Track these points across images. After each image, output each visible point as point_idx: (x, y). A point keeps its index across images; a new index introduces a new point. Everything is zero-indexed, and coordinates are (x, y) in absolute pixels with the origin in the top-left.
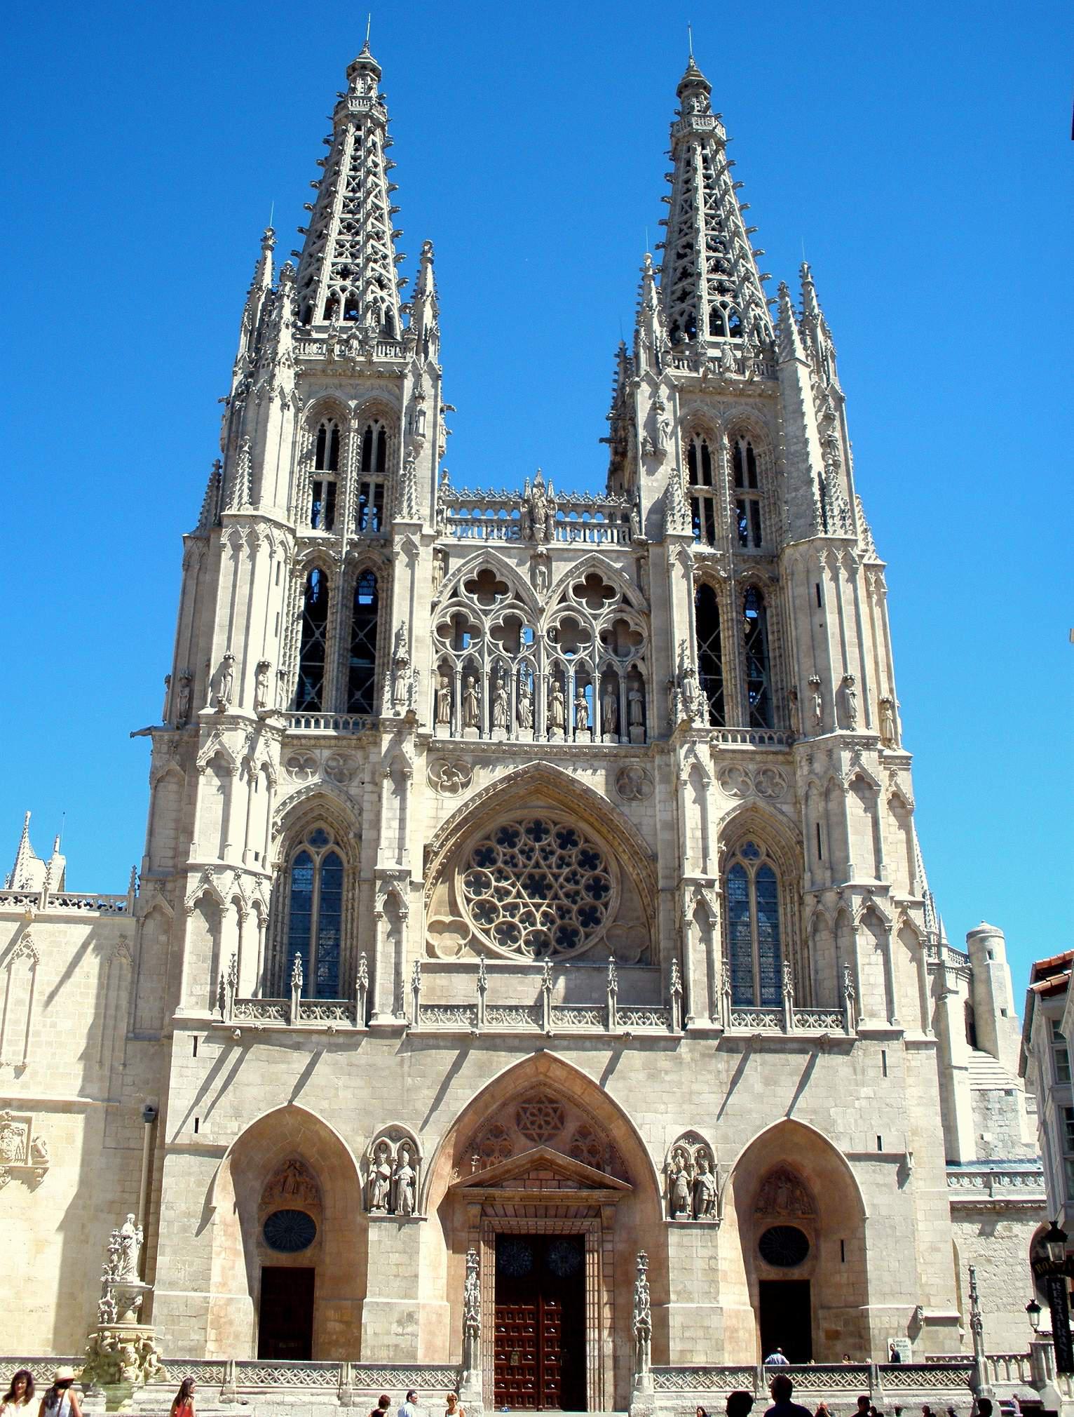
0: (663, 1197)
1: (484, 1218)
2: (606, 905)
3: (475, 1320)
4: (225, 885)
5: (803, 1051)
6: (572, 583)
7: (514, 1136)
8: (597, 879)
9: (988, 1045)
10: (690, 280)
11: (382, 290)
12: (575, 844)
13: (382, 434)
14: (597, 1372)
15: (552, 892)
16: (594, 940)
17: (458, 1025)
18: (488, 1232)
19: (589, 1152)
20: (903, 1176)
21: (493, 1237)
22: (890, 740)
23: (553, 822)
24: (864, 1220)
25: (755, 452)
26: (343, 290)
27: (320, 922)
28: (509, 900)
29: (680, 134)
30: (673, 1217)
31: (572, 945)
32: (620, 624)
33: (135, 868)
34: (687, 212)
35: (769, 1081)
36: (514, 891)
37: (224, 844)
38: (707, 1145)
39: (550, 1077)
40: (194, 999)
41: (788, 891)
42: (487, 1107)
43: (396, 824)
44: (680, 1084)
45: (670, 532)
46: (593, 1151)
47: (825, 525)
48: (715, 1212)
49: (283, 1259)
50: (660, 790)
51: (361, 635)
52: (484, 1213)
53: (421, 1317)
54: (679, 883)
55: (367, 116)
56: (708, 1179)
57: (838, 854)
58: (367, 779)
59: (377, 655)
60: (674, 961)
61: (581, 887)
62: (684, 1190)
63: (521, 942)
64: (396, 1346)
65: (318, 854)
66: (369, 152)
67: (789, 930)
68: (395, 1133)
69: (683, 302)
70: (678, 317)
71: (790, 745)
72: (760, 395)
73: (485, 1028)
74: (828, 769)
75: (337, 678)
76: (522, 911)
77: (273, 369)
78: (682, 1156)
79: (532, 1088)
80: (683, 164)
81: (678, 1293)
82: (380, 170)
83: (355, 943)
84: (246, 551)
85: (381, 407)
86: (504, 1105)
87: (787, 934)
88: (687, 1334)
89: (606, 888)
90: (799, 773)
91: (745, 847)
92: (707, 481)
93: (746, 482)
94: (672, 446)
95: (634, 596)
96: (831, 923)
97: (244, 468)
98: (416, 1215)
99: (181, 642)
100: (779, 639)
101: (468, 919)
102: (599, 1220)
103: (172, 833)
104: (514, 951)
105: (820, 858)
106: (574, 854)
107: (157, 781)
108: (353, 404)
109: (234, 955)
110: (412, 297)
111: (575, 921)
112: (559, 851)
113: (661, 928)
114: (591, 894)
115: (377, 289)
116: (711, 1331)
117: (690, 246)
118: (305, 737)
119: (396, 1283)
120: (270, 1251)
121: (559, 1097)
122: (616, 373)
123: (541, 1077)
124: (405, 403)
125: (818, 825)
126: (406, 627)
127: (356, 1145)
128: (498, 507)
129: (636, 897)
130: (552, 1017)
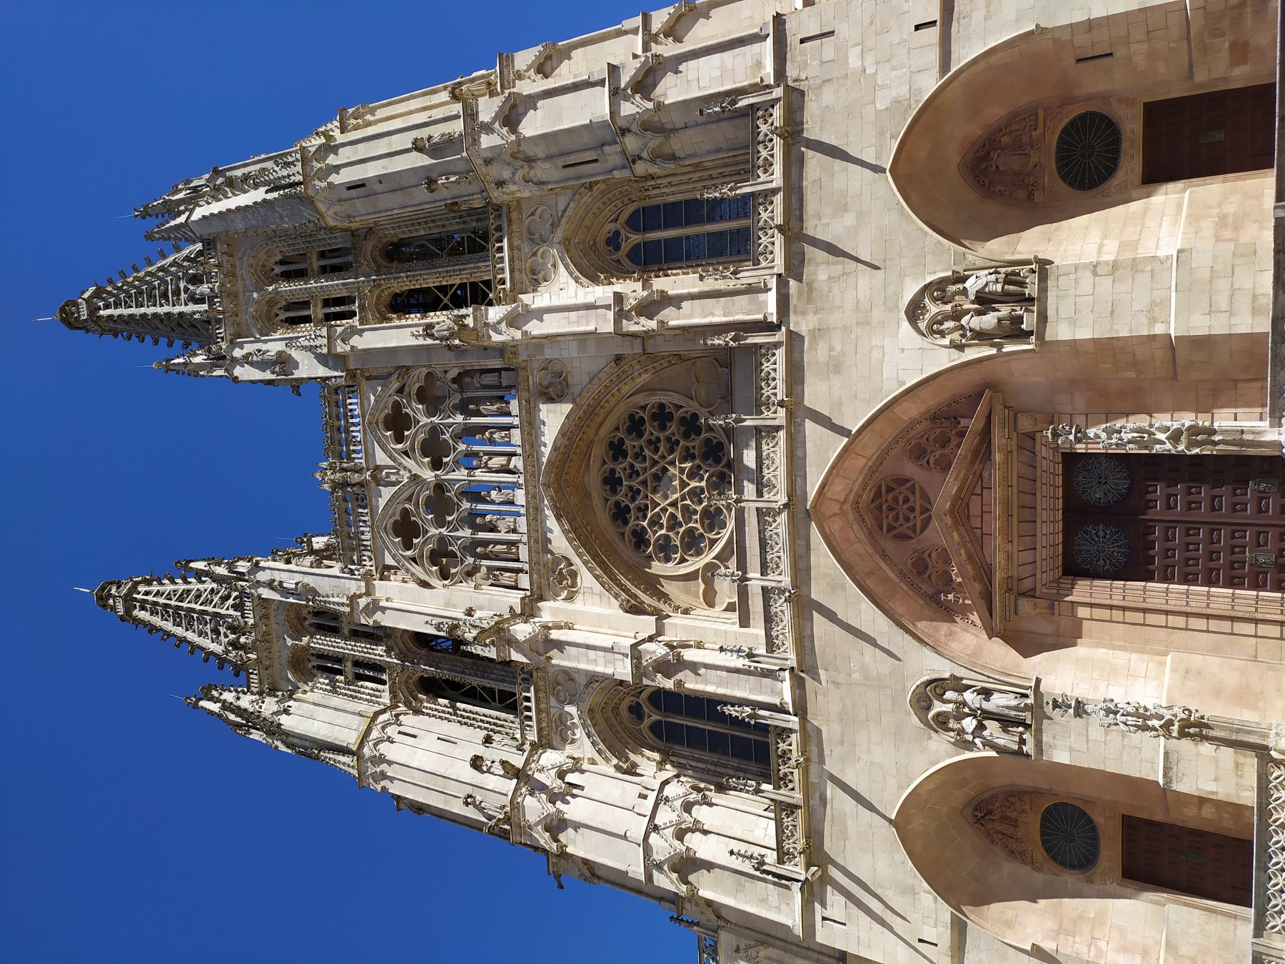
0: (999, 350)
1: (1038, 594)
4: (663, 846)
5: (801, 160)
6: (392, 445)
8: (654, 417)
12: (621, 441)
21: (1068, 580)
23: (603, 465)
30: (1031, 333)
32: (422, 396)
38: (926, 287)
39: (846, 500)
40: (783, 907)
41: (648, 193)
48: (1024, 270)
49: (1111, 852)
50: (549, 353)
52: (1031, 594)
56: (972, 285)
57: (586, 139)
62: (989, 321)
73: (786, 581)
76: (688, 502)
81: (1153, 321)
84: (384, 767)
86: (884, 555)
88: (1224, 305)
89: (662, 406)
91: (611, 248)
100: (419, 224)
105: (596, 161)
108: (289, 642)
112: (629, 459)
114: (668, 424)
121: (872, 484)
123: (847, 507)
125: (564, 167)
126: (429, 618)
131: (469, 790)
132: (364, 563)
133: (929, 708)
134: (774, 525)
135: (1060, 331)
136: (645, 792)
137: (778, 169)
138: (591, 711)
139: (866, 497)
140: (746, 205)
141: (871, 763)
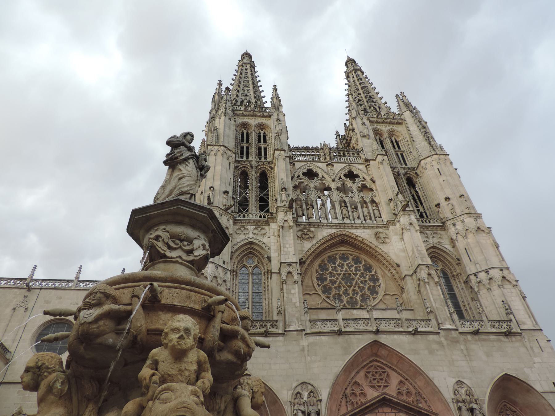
2: (379, 286)
13: (264, 133)
15: (355, 281)
16: (377, 301)
25: (398, 140)
28: (336, 285)
35: (488, 355)
36: (338, 281)
38: (470, 388)
42: (350, 373)
58: (272, 234)
61: (367, 279)
63: (345, 302)
65: (250, 267)
79: (371, 362)
89: (378, 280)
90: (450, 231)
96: (488, 286)
101: (320, 293)
112: (355, 266)
121: (384, 367)
125: (465, 249)
128: (311, 151)
129: (391, 283)
132: (293, 156)
134: (364, 325)
137: (493, 330)
138: (251, 243)
141: (270, 364)
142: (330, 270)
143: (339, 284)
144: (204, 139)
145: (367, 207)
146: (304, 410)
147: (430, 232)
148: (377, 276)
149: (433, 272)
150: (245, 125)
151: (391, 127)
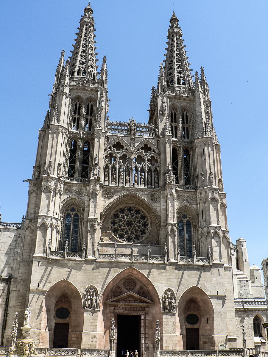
2: (147, 229)
3: (113, 338)
4: (48, 221)
7: (123, 289)
8: (145, 222)
9: (242, 269)
10: (172, 70)
11: (92, 68)
12: (140, 213)
13: (92, 106)
14: (143, 352)
16: (144, 238)
17: (108, 259)
18: (116, 314)
19: (142, 293)
20: (224, 301)
22: (221, 189)
24: (213, 313)
26: (82, 68)
27: (72, 232)
29: (171, 32)
30: (164, 311)
31: (138, 239)
32: (152, 157)
33: (23, 216)
34: (172, 52)
35: (189, 276)
37: (48, 211)
39: (133, 274)
40: (39, 251)
41: (194, 227)
42: (116, 281)
43: (94, 206)
44: (166, 276)
45: (166, 134)
46: (144, 293)
47: (206, 134)
49: (61, 321)
50: (162, 200)
51: (85, 158)
52: (115, 309)
53: (98, 336)
54: (167, 224)
55: (89, 22)
56: (173, 301)
57: (208, 218)
58: (86, 195)
59: (89, 163)
60: (165, 244)
62: (167, 304)
63: (125, 238)
64: (91, 344)
65: (73, 214)
66: (90, 32)
67: (194, 237)
68: (92, 288)
69: (170, 76)
70: (169, 80)
71: (196, 190)
72: (189, 100)
73: (116, 260)
74: (205, 196)
75: (79, 168)
76: (125, 230)
77: (64, 87)
78: (167, 295)
79: (128, 276)
80: (171, 40)
82: (92, 37)
83: (82, 237)
85: (92, 99)
86: (120, 281)
87: (194, 238)
88: (167, 342)
89: (147, 225)
90: (198, 197)
92: (175, 122)
93: (185, 122)
94: (166, 112)
95: (156, 150)
96: (206, 236)
97: (55, 113)
98: (97, 309)
99: (38, 157)
100: (193, 163)
102: (145, 311)
103: (34, 207)
104: (123, 240)
105: (203, 219)
106: (139, 216)
107: (30, 193)
109: (50, 240)
110: (100, 70)
111: (139, 233)
113: (162, 235)
115: (91, 68)
116: (174, 341)
117: (172, 61)
118: (70, 183)
119: (91, 327)
120: (57, 319)
122: (151, 94)
124: (98, 98)
125: (202, 210)
127: (82, 291)
129: (155, 228)
130: (134, 258)
131: (53, 162)
133: (91, 289)
135: (164, 317)
136: (58, 214)
138: (74, 199)
139: (132, 277)
140: (191, 255)
142: (120, 218)
143: (124, 227)
144: (48, 111)
145: (151, 175)
146: (90, 298)
147: (186, 195)
148: (147, 223)
149: (175, 228)
150: (78, 98)
151: (184, 103)
